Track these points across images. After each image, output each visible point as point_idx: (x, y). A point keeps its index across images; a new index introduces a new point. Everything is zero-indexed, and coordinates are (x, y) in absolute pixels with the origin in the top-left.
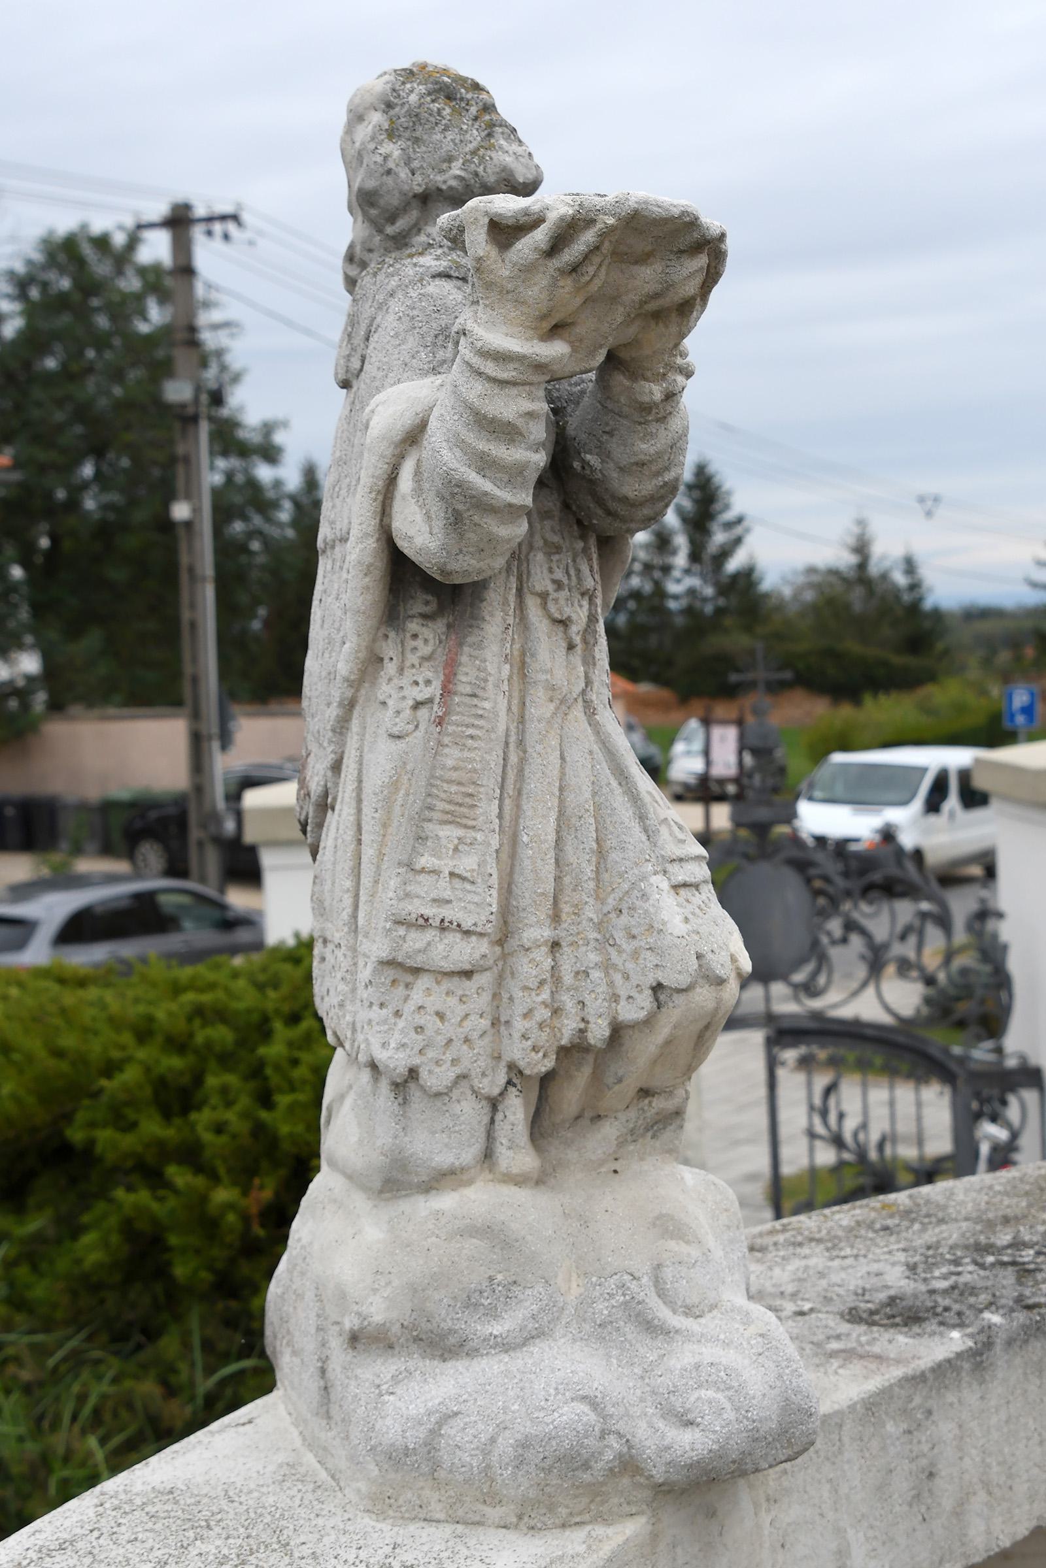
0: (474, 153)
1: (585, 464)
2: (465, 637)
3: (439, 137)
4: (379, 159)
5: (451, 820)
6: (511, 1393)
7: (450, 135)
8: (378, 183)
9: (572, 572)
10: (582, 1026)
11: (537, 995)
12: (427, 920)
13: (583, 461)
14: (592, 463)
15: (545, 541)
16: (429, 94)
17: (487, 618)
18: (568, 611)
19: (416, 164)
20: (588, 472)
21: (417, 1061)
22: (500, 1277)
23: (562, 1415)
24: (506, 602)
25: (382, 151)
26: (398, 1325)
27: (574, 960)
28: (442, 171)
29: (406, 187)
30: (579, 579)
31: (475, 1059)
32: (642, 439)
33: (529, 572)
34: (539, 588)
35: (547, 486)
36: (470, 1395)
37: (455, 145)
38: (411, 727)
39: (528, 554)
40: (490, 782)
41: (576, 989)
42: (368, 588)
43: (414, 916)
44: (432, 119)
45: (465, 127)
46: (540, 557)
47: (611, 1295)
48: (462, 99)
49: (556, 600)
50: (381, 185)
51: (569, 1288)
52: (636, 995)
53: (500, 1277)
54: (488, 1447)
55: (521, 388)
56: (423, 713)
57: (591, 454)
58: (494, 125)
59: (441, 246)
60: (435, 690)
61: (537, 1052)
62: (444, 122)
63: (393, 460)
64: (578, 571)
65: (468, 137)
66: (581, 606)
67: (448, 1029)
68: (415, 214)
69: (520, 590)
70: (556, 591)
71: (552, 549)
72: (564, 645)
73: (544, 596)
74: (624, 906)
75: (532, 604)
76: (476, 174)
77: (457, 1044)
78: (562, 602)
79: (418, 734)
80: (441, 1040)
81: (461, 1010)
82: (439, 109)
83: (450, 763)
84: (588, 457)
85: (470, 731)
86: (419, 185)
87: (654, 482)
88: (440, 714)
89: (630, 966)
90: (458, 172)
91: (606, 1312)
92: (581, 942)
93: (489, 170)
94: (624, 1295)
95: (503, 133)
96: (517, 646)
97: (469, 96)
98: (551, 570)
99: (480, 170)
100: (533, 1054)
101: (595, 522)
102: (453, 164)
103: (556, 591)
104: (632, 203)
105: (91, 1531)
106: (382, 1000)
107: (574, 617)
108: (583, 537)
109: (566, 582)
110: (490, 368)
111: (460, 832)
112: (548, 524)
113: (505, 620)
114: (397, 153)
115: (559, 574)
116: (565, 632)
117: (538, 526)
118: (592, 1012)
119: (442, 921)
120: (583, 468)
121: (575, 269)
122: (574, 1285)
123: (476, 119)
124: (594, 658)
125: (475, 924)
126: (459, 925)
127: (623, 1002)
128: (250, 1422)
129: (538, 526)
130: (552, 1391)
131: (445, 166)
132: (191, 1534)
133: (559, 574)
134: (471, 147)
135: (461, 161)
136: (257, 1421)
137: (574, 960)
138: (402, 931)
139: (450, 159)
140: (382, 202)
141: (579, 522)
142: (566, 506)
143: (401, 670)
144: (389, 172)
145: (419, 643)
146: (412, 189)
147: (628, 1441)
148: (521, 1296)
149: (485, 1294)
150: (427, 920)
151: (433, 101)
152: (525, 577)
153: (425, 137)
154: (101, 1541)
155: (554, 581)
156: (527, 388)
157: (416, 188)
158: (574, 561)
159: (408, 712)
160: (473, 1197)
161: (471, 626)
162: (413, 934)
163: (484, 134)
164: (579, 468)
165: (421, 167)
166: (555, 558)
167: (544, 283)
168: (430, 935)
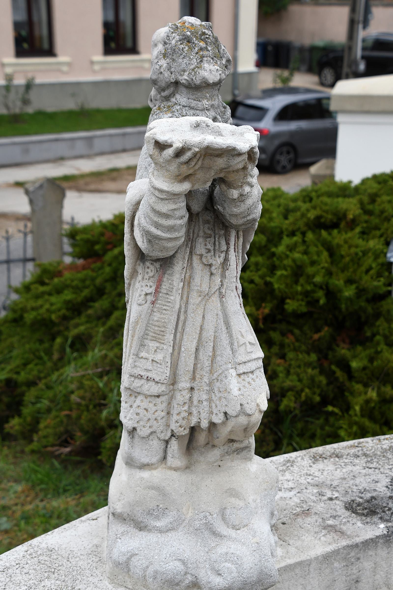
0: (193, 70)
2: (166, 271)
3: (181, 60)
4: (158, 67)
5: (155, 339)
6: (156, 551)
7: (185, 61)
8: (157, 77)
10: (199, 420)
11: (183, 407)
12: (142, 376)
14: (220, 209)
15: (205, 233)
16: (180, 41)
17: (176, 264)
18: (211, 261)
19: (173, 70)
21: (135, 425)
22: (161, 506)
23: (169, 566)
24: (184, 258)
26: (126, 514)
27: (198, 396)
28: (181, 75)
29: (168, 80)
30: (219, 247)
31: (158, 426)
32: (235, 207)
33: (195, 246)
34: (198, 253)
35: (209, 210)
36: (143, 548)
37: (187, 65)
38: (144, 302)
39: (196, 239)
40: (171, 327)
41: (198, 407)
42: (129, 250)
43: (137, 375)
44: (180, 52)
45: (192, 57)
46: (201, 240)
47: (201, 519)
48: (193, 43)
49: (206, 257)
50: (158, 78)
51: (188, 513)
52: (219, 414)
53: (161, 506)
54: (146, 569)
55: (169, 200)
56: (149, 297)
58: (204, 57)
59: (180, 105)
60: (152, 290)
61: (182, 428)
62: (184, 54)
63: (133, 210)
65: (192, 62)
66: (219, 257)
67: (149, 415)
68: (172, 89)
69: (191, 253)
72: (209, 274)
73: (201, 256)
74: (219, 379)
75: (196, 259)
76: (192, 80)
77: (151, 421)
78: (209, 258)
79: (146, 305)
80: (146, 419)
81: (154, 409)
82: (183, 48)
83: (156, 319)
84: (218, 207)
85: (165, 307)
86: (173, 79)
87: (243, 220)
88: (153, 300)
89: (218, 402)
90: (186, 78)
91: (198, 525)
92: (202, 390)
93: (197, 79)
94: (206, 520)
95: (207, 60)
96: (188, 274)
97: (196, 42)
98: (206, 245)
99: (194, 78)
100: (180, 428)
104: (206, 144)
105: (17, 564)
106: (126, 400)
107: (214, 263)
110: (157, 193)
111: (158, 345)
113: (183, 265)
114: (165, 65)
115: (209, 246)
116: (210, 269)
118: (202, 417)
119: (148, 377)
121: (187, 162)
122: (190, 512)
123: (197, 53)
124: (225, 275)
125: (160, 380)
126: (154, 379)
127: (214, 415)
128: (96, 519)
129: (202, 227)
130: (168, 556)
131: (182, 73)
132: (46, 575)
134: (192, 67)
136: (98, 519)
137: (198, 396)
138: (133, 379)
139: (184, 71)
140: (159, 84)
143: (143, 279)
144: (161, 73)
145: (149, 270)
146: (170, 80)
147: (196, 577)
148: (168, 514)
149: (155, 511)
150: (142, 376)
151: (181, 44)
153: (176, 59)
154: (17, 571)
155: (207, 249)
156: (173, 200)
157: (172, 80)
158: (219, 239)
159: (143, 296)
160: (155, 474)
161: (169, 267)
162: (137, 380)
163: (198, 61)
165: (175, 71)
167: (175, 166)
168: (143, 382)
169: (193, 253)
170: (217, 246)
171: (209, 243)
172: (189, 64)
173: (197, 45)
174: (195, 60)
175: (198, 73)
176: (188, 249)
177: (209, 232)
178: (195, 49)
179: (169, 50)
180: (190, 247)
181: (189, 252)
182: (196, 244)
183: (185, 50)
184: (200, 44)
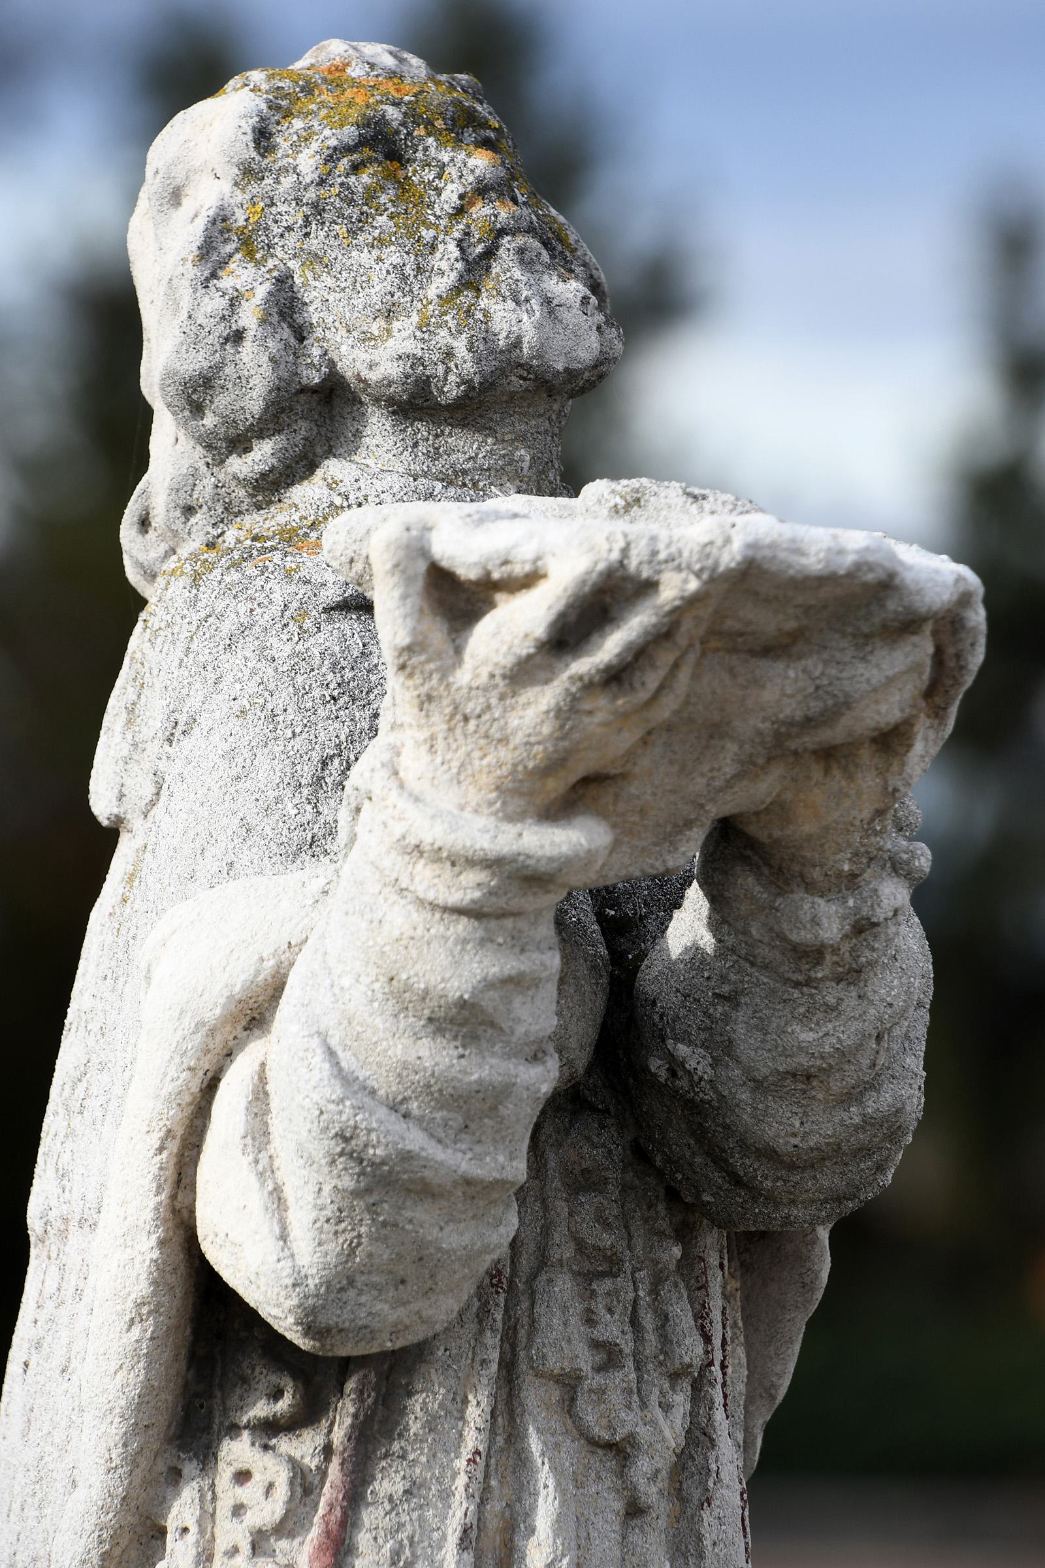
1: (675, 1067)
9: (648, 1321)
13: (671, 1057)
14: (691, 1064)
20: (683, 1083)
25: (226, 282)
33: (533, 1322)
34: (554, 1363)
37: (404, 278)
39: (533, 1276)
45: (427, 234)
46: (564, 1286)
57: (690, 1043)
64: (664, 1319)
70: (600, 1369)
71: (597, 1267)
76: (449, 354)
84: (682, 1050)
97: (445, 157)
98: (590, 1320)
101: (707, 1198)
102: (396, 325)
103: (600, 1369)
108: (684, 1233)
109: (627, 1347)
112: (589, 1202)
114: (262, 291)
115: (613, 1329)
117: (561, 1207)
120: (673, 1073)
129: (561, 1207)
133: (613, 1329)
135: (415, 318)
141: (673, 1195)
142: (640, 1155)
152: (522, 1333)
155: (596, 1345)
158: (654, 1291)
164: (663, 1075)
166: (604, 1286)
169: (523, 1367)
170: (651, 1337)
171: (610, 1311)
172: (419, 270)
173: (452, 171)
174: (452, 248)
175: (479, 316)
176: (492, 1341)
177: (607, 1240)
178: (439, 191)
179: (283, 208)
180: (499, 1325)
181: (495, 1355)
182: (540, 1309)
183: (383, 199)
184: (471, 162)
